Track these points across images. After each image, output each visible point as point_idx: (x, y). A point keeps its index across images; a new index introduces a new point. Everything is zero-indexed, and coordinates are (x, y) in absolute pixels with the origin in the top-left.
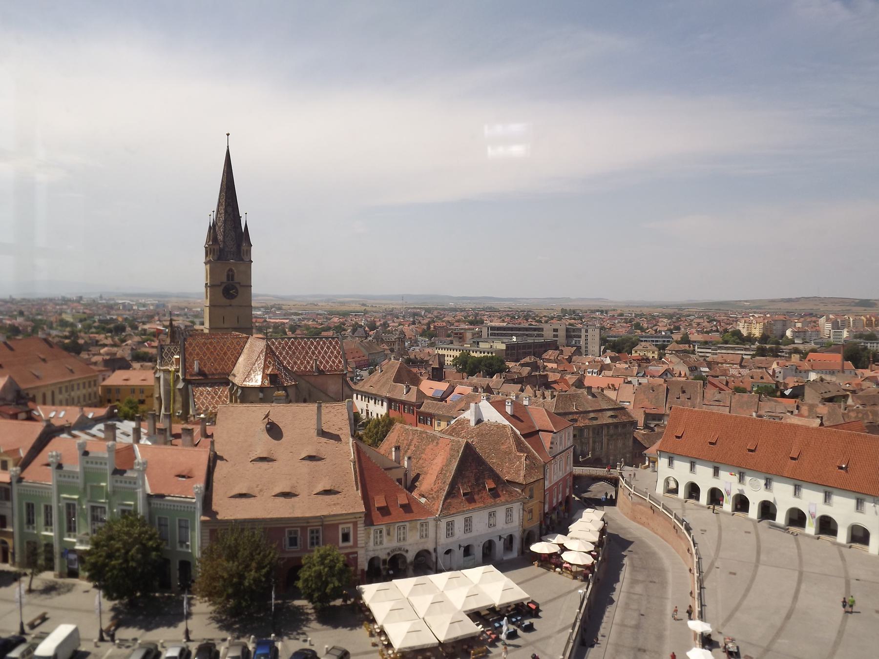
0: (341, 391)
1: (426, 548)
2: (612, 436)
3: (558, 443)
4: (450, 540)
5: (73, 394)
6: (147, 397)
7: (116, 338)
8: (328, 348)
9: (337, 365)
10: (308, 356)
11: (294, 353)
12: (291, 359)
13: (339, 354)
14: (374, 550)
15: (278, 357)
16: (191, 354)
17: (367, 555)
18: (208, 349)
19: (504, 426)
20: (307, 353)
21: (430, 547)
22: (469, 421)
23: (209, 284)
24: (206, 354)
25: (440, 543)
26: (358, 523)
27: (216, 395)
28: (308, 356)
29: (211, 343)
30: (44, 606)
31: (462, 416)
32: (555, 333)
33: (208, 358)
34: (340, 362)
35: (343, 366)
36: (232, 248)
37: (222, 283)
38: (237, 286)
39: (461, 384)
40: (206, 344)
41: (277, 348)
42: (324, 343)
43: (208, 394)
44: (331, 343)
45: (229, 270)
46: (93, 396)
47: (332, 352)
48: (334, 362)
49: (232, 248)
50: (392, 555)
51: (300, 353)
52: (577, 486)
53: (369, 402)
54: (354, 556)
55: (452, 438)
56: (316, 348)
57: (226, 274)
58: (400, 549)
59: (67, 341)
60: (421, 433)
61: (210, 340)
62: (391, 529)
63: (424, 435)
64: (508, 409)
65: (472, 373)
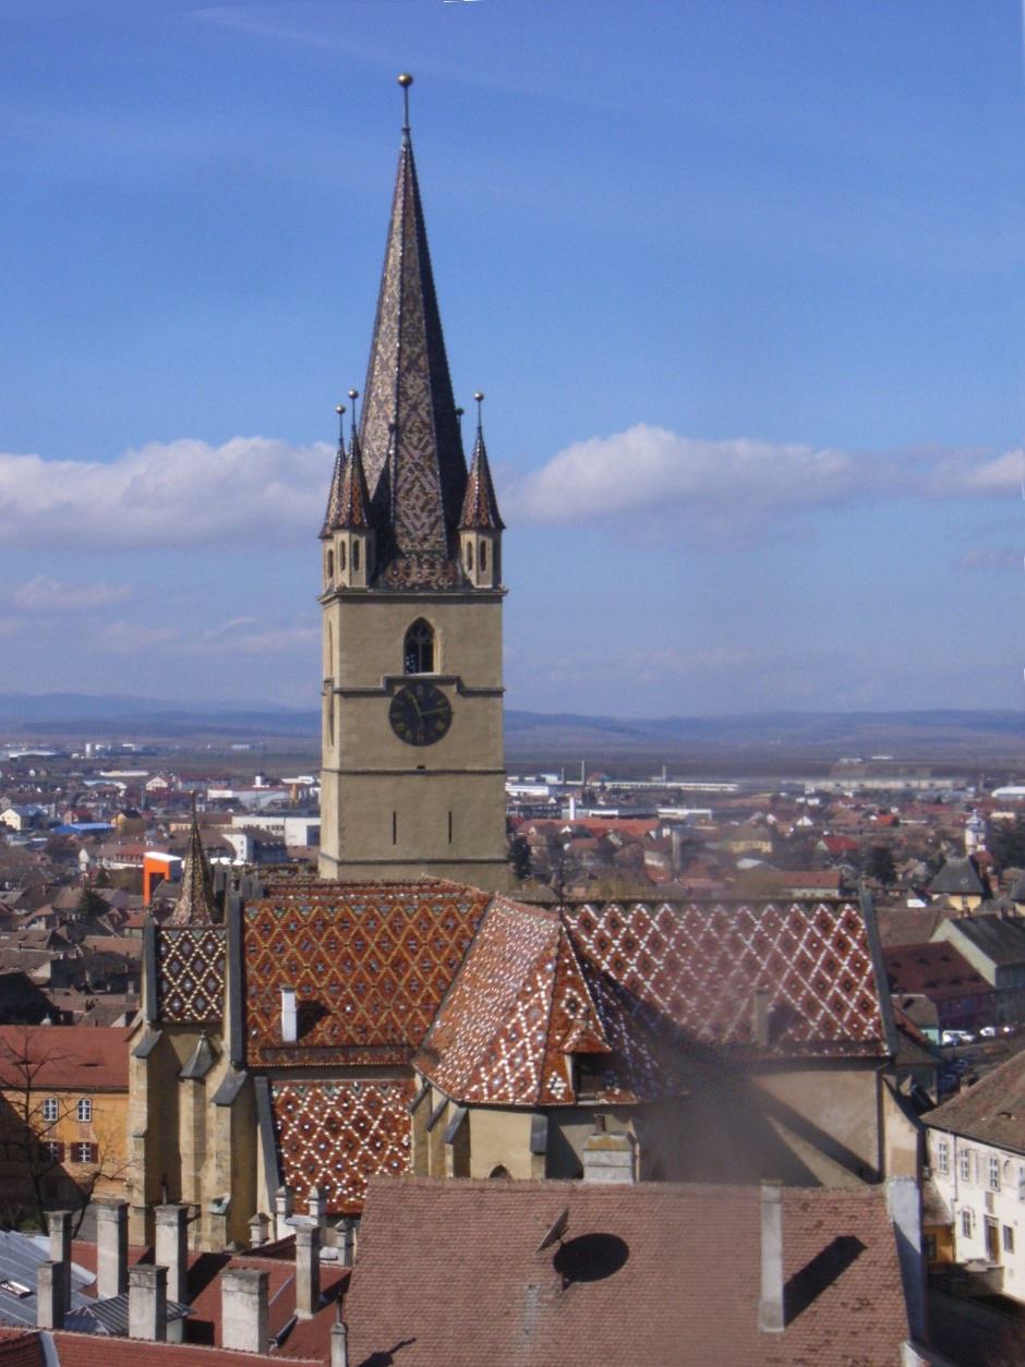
8: (815, 945)
9: (853, 1018)
11: (672, 965)
16: (266, 966)
18: (333, 945)
20: (725, 965)
23: (337, 685)
24: (327, 967)
27: (364, 1132)
29: (344, 922)
33: (334, 981)
34: (865, 1006)
35: (877, 1025)
36: (425, 539)
38: (450, 691)
40: (325, 925)
41: (603, 944)
42: (798, 925)
44: (825, 925)
47: (831, 965)
48: (838, 1006)
49: (425, 539)
56: (761, 943)
61: (339, 911)
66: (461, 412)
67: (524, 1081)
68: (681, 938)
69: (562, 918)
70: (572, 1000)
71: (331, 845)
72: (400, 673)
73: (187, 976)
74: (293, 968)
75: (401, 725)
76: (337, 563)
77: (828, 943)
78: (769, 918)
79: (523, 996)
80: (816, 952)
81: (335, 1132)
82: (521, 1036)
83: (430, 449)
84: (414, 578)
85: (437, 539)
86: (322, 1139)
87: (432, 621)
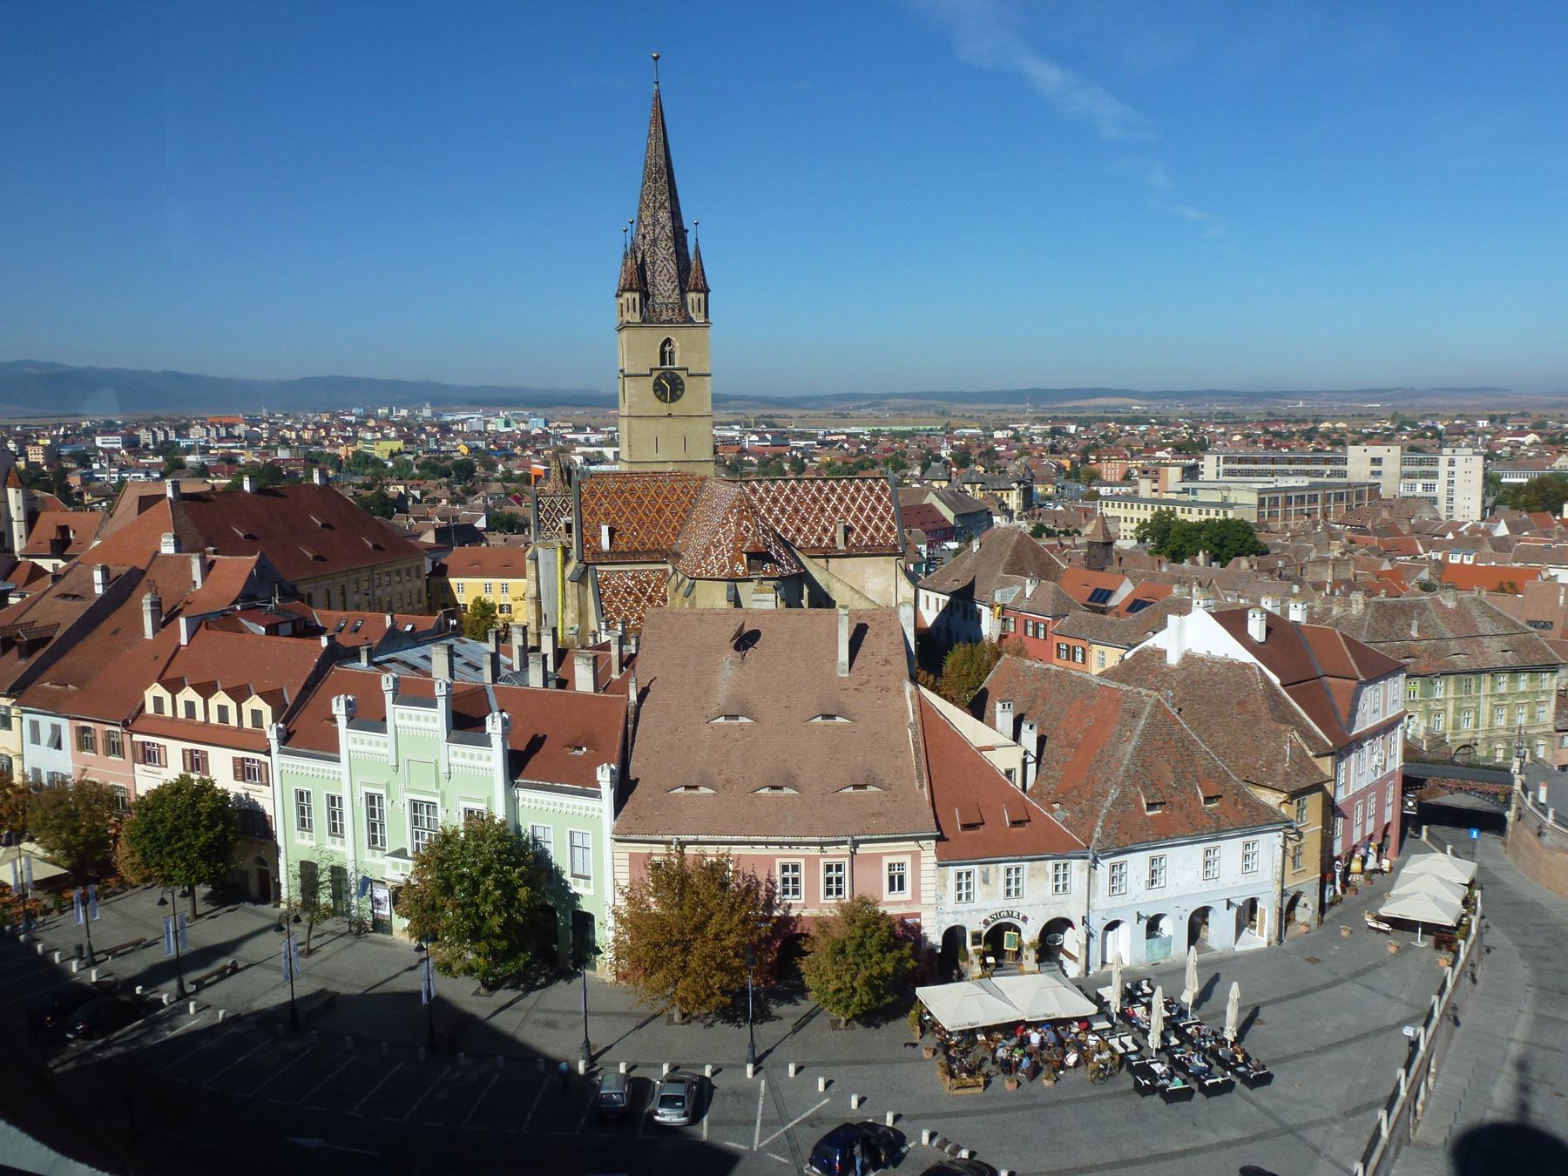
1: (1065, 916)
2: (1502, 696)
4: (1118, 901)
7: (458, 488)
10: (823, 516)
11: (796, 510)
12: (791, 524)
13: (888, 512)
15: (763, 518)
16: (593, 513)
17: (939, 922)
18: (626, 502)
19: (1245, 666)
20: (822, 510)
23: (626, 372)
27: (644, 594)
28: (823, 516)
29: (632, 490)
31: (1149, 643)
32: (1376, 468)
33: (627, 520)
34: (890, 529)
35: (896, 538)
36: (670, 297)
37: (652, 370)
38: (683, 375)
40: (622, 492)
41: (762, 500)
42: (858, 490)
43: (627, 592)
44: (871, 489)
47: (874, 509)
48: (877, 529)
49: (670, 297)
51: (809, 510)
55: (1125, 687)
56: (841, 500)
59: (369, 493)
60: (1058, 674)
64: (1256, 629)
66: (687, 231)
67: (723, 567)
68: (800, 497)
69: (741, 487)
70: (747, 527)
73: (554, 519)
74: (607, 514)
75: (659, 393)
76: (625, 309)
77: (872, 498)
78: (844, 487)
79: (722, 525)
80: (867, 503)
81: (630, 594)
82: (721, 545)
83: (672, 250)
84: (664, 317)
85: (675, 297)
86: (623, 597)
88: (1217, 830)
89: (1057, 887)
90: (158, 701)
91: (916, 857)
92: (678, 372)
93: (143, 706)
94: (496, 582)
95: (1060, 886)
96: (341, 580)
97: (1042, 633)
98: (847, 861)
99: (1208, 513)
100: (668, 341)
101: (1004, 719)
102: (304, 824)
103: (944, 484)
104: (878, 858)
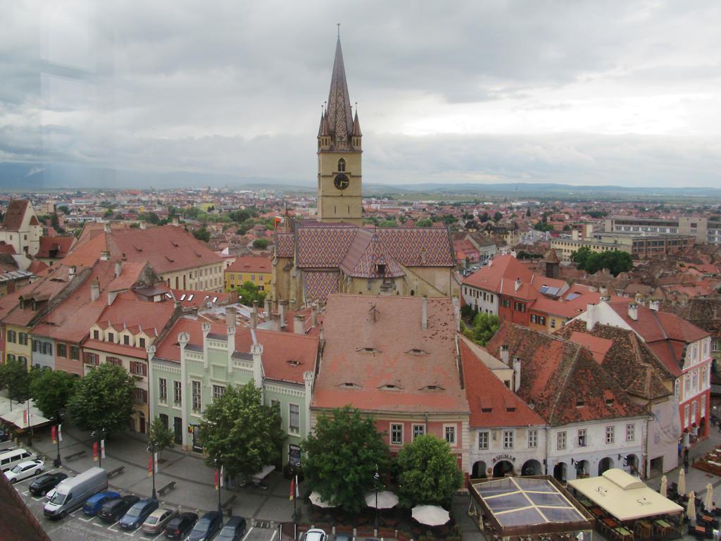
0: (449, 285)
3: (691, 356)
4: (562, 453)
5: (201, 279)
6: (266, 284)
14: (479, 454)
17: (471, 459)
19: (626, 333)
21: (539, 457)
22: (585, 323)
25: (550, 455)
26: (463, 423)
30: (174, 477)
39: (579, 282)
45: (340, 160)
46: (218, 280)
50: (498, 461)
52: (715, 407)
53: (478, 297)
54: (458, 457)
57: (337, 164)
58: (506, 457)
60: (531, 332)
62: (498, 433)
63: (535, 336)
65: (591, 271)
71: (320, 215)
72: (337, 171)
76: (321, 144)
87: (345, 159)
88: (613, 416)
89: (531, 444)
90: (96, 333)
91: (460, 424)
92: (347, 175)
93: (89, 335)
94: (257, 275)
95: (533, 444)
96: (184, 273)
97: (523, 309)
98: (425, 425)
99: (607, 249)
100: (342, 160)
101: (504, 355)
102: (163, 396)
103: (475, 230)
104: (440, 424)
